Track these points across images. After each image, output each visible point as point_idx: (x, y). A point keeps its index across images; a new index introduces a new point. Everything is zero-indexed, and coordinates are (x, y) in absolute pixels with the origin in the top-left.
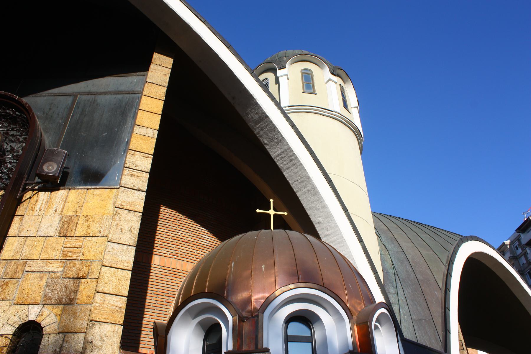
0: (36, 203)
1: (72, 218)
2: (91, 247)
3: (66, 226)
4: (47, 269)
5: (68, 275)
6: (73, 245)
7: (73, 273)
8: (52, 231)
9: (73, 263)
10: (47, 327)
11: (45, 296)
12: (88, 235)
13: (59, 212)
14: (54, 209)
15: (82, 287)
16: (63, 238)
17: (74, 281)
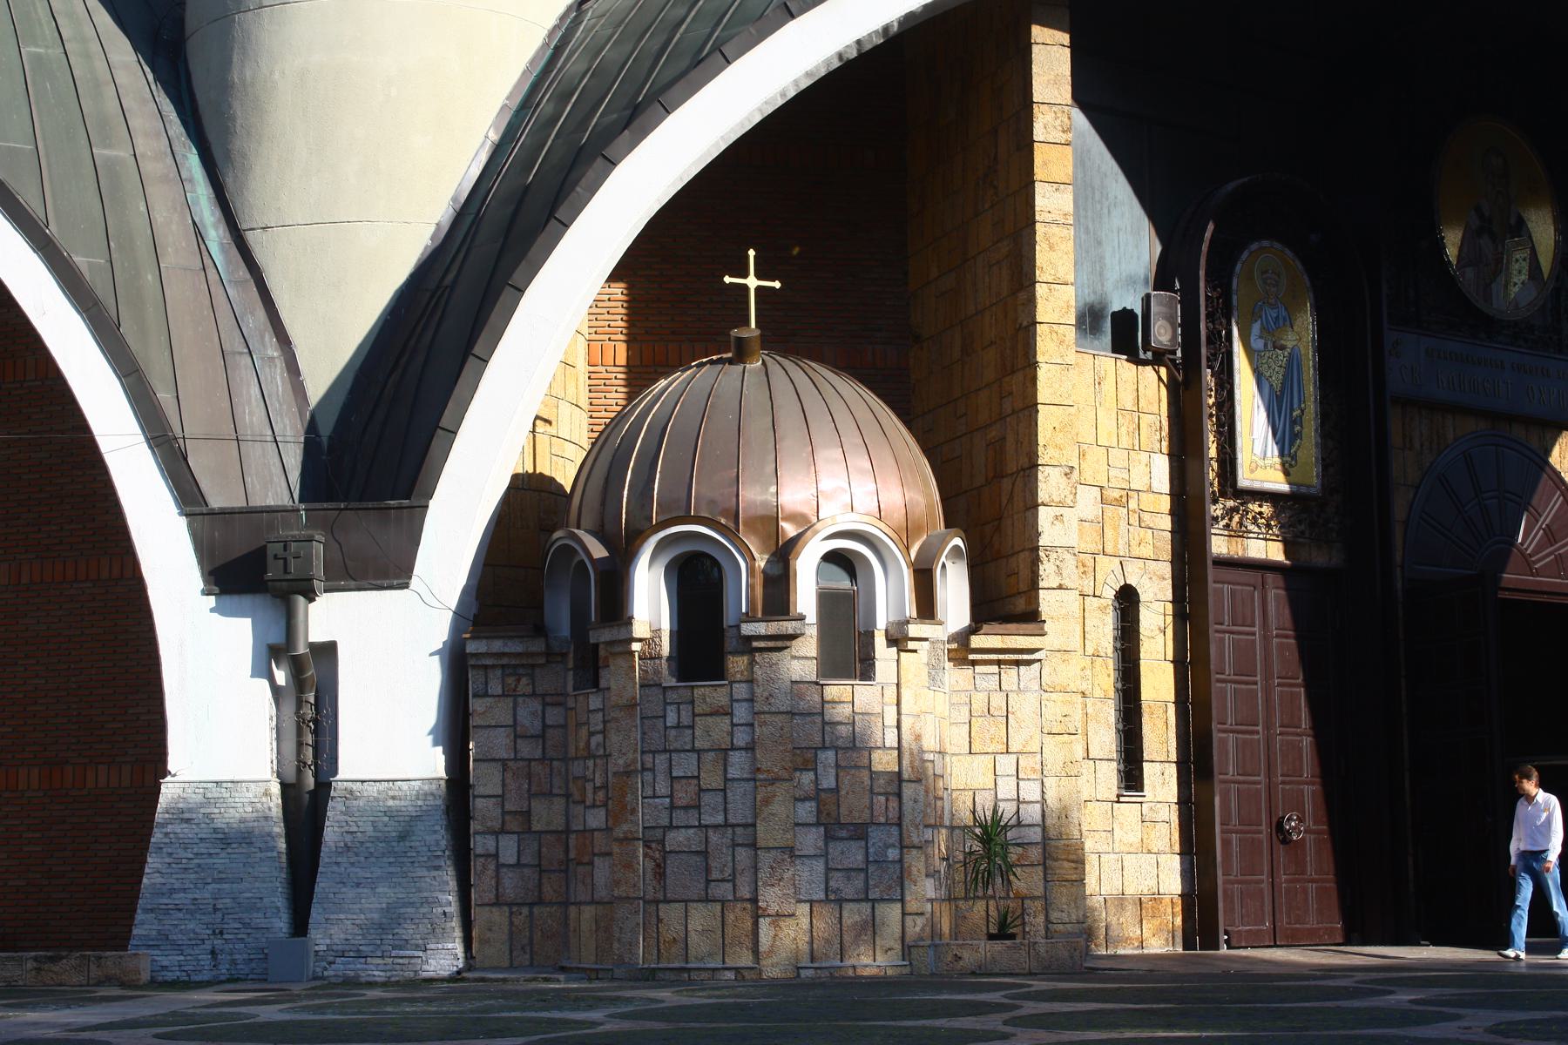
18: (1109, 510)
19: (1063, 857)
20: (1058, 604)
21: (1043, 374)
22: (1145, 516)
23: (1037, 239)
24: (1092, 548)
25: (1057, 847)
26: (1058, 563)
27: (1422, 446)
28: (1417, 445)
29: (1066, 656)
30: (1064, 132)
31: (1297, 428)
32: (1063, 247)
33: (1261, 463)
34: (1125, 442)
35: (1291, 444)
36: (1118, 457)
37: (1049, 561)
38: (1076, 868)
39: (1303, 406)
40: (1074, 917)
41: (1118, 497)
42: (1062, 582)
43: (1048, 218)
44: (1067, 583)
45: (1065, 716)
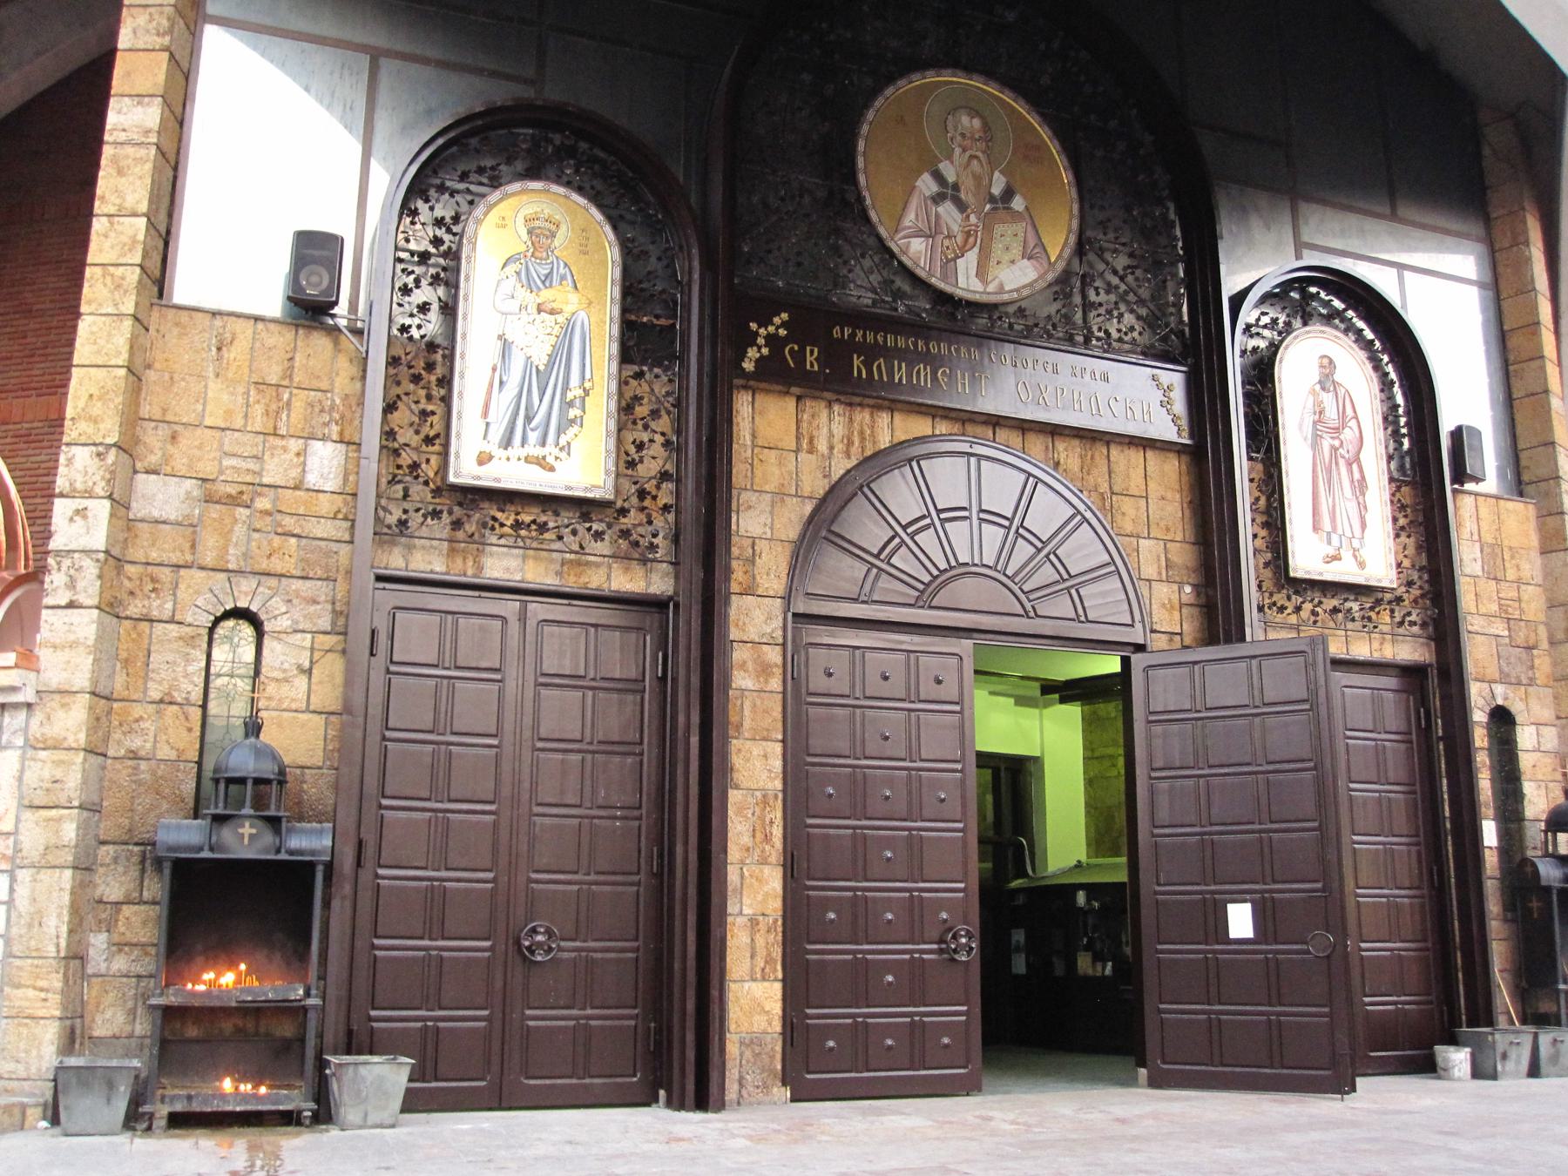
7: (1520, 640)
11: (1501, 672)
13: (1476, 537)
15: (1537, 662)
18: (215, 511)
19: (28, 983)
20: (66, 627)
21: (84, 327)
22: (289, 523)
23: (103, 162)
24: (175, 558)
25: (20, 968)
26: (72, 572)
27: (831, 448)
28: (822, 446)
29: (67, 699)
30: (158, 34)
31: (573, 413)
32: (137, 170)
33: (499, 453)
34: (258, 423)
35: (560, 431)
36: (249, 444)
37: (59, 569)
38: (45, 1000)
39: (587, 385)
40: (33, 1070)
41: (234, 492)
42: (74, 598)
43: (122, 137)
44: (82, 598)
45: (56, 782)
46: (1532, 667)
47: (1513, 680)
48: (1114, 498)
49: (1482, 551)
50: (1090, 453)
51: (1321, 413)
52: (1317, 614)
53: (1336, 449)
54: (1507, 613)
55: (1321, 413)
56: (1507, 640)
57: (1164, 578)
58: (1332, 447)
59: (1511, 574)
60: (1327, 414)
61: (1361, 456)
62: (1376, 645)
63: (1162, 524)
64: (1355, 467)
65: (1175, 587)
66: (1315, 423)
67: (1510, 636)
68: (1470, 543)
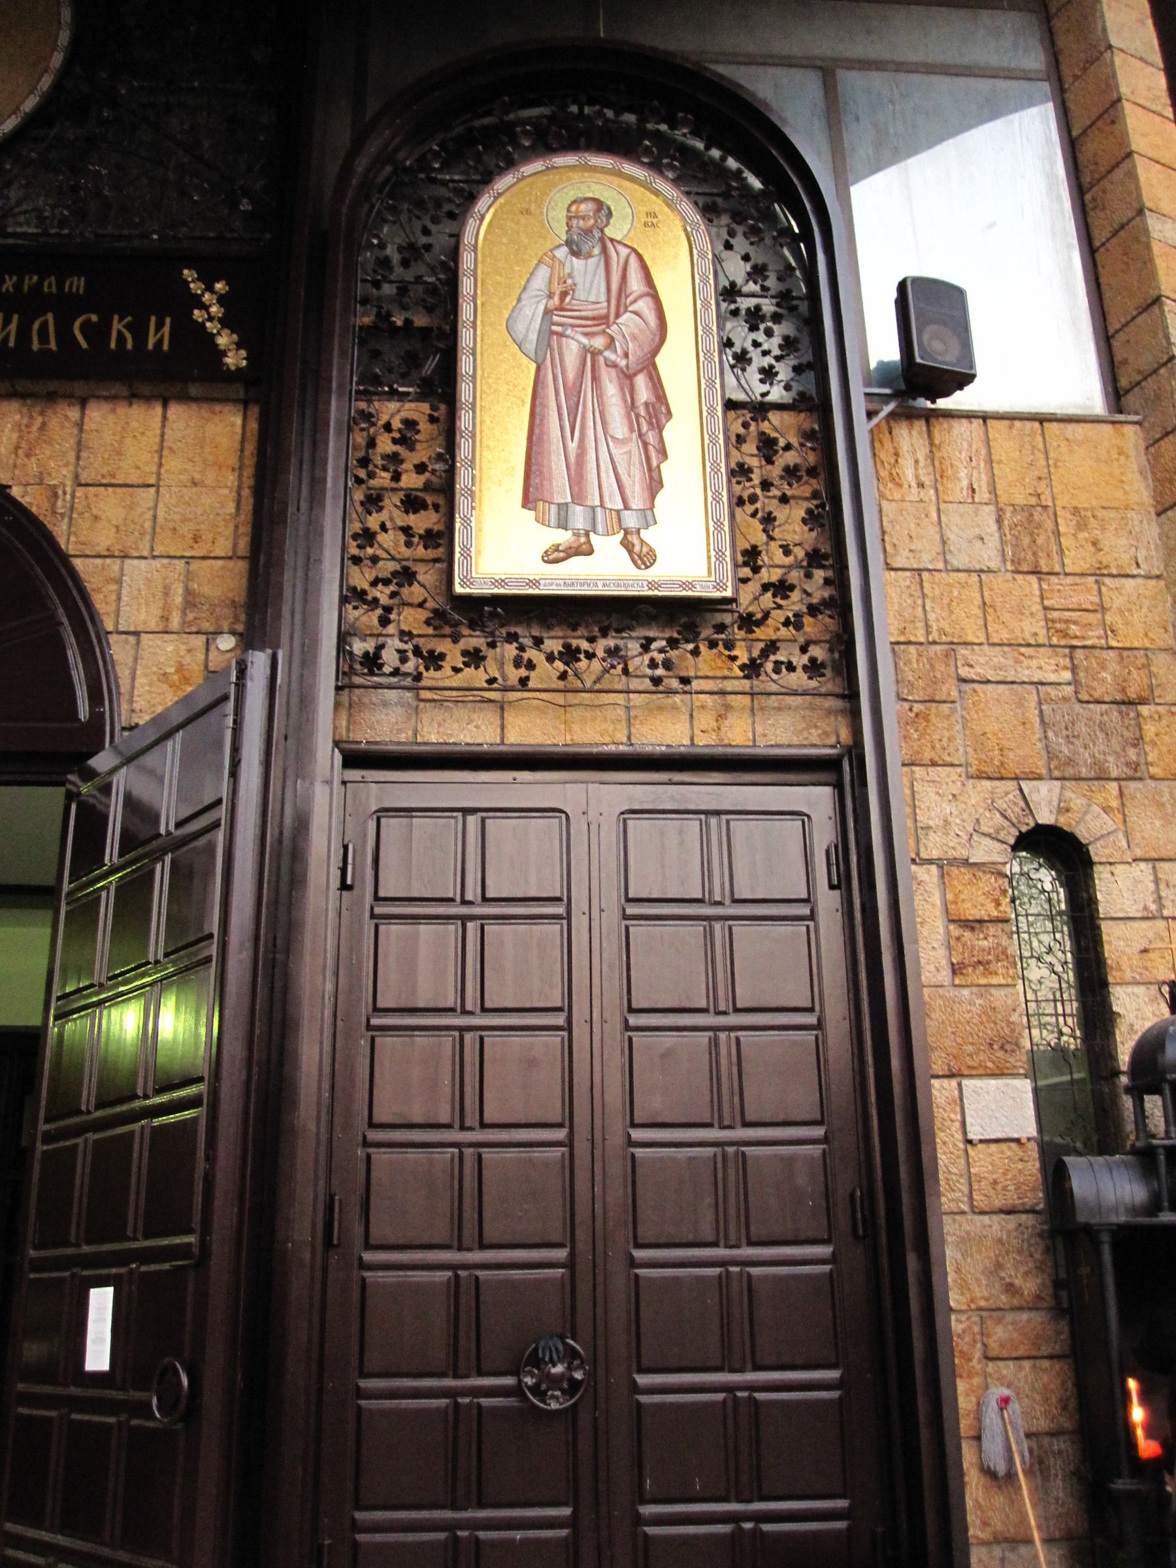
0: (897, 461)
1: (1031, 515)
2: (1130, 610)
3: (1026, 540)
4: (1024, 675)
5: (1097, 695)
6: (1075, 600)
8: (988, 555)
9: (1096, 658)
10: (1099, 844)
11: (1051, 755)
12: (1105, 572)
13: (983, 495)
14: (965, 483)
15: (1150, 730)
16: (1033, 579)
17: (1120, 712)
46: (1138, 742)
47: (1084, 772)
48: (80, 492)
49: (999, 521)
50: (39, 420)
51: (564, 294)
52: (531, 666)
53: (595, 354)
54: (1065, 634)
55: (564, 294)
56: (1069, 690)
57: (175, 622)
58: (585, 350)
59: (1077, 558)
60: (581, 294)
61: (659, 360)
62: (705, 720)
63: (186, 529)
64: (641, 381)
65: (200, 641)
66: (547, 312)
67: (1075, 682)
68: (969, 509)
